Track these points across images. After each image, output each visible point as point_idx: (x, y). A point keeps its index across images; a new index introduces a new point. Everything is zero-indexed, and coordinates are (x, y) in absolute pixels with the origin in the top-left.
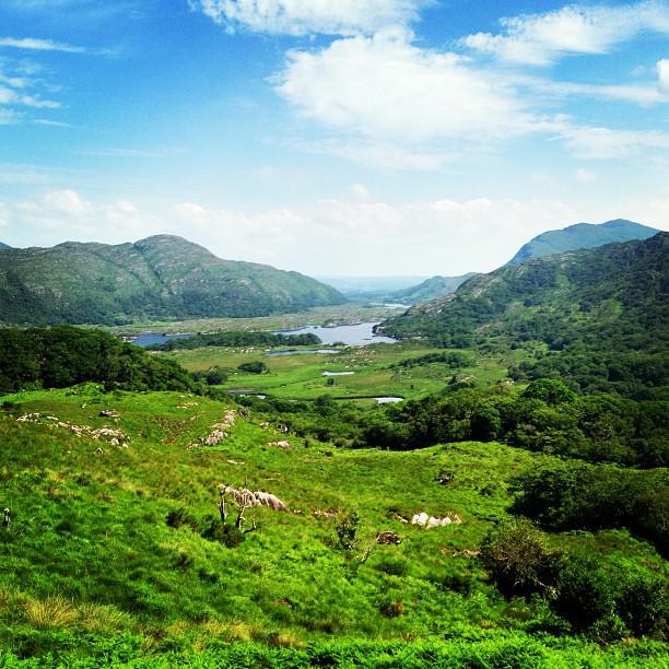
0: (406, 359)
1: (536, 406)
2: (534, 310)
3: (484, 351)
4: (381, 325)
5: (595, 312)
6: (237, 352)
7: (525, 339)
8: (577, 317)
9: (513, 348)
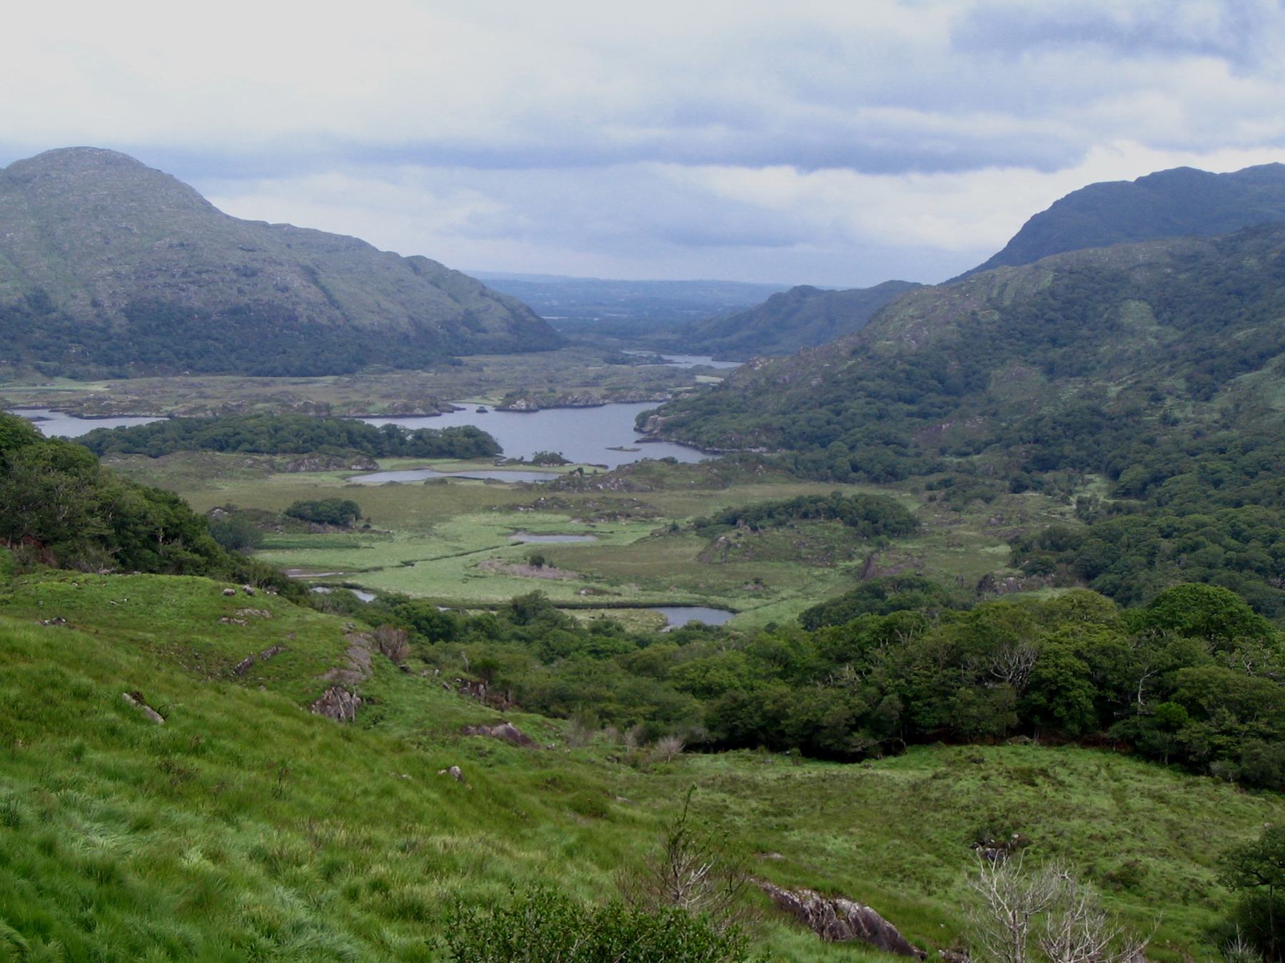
0: (737, 506)
1: (1185, 659)
2: (1070, 390)
3: (940, 494)
4: (658, 412)
5: (1222, 401)
6: (275, 469)
7: (1046, 464)
8: (1177, 414)
9: (1018, 488)
